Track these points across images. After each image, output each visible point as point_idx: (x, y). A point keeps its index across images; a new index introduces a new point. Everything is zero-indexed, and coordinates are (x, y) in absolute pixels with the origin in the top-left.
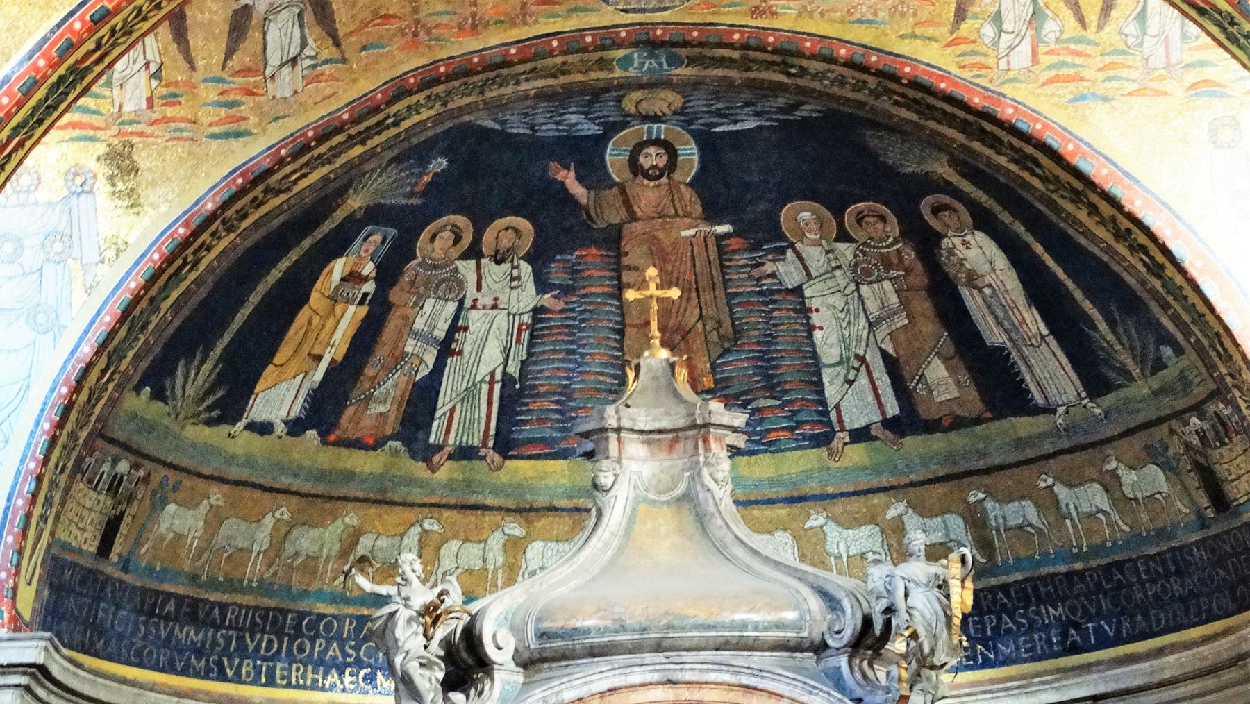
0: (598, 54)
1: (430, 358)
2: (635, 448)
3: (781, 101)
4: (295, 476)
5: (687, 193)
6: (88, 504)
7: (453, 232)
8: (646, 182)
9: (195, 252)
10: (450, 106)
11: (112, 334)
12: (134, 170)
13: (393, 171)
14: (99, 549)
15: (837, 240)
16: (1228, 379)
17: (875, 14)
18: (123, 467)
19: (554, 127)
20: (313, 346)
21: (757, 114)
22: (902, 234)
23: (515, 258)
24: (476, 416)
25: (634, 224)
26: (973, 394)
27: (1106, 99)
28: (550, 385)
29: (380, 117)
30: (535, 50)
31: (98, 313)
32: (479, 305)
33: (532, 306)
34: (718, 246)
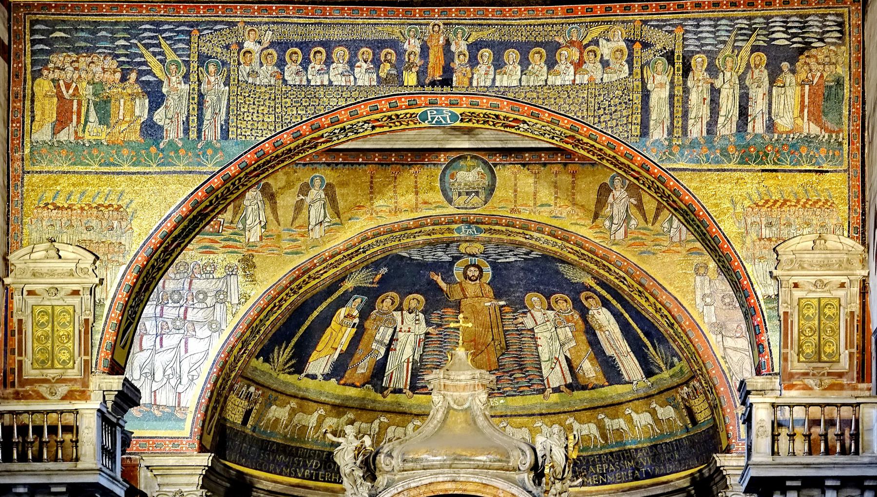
0: (447, 226)
1: (383, 351)
3: (524, 250)
4: (327, 396)
5: (488, 288)
6: (237, 404)
9: (279, 301)
10: (387, 245)
11: (243, 334)
13: (364, 273)
14: (242, 422)
15: (548, 309)
16: (698, 371)
17: (561, 214)
18: (252, 389)
21: (515, 255)
22: (574, 308)
26: (601, 376)
27: (654, 254)
29: (356, 249)
30: (420, 223)
31: (237, 325)
32: (403, 330)
34: (501, 311)
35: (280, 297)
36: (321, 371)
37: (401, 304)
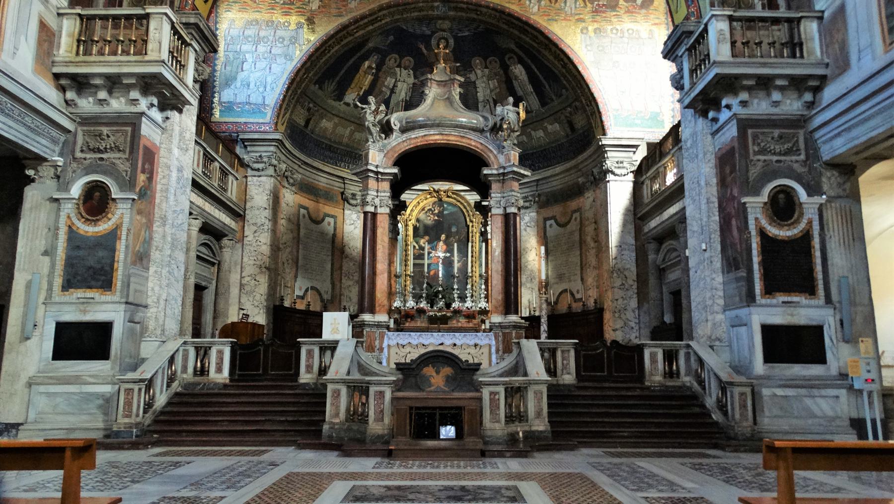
1: (388, 94)
2: (434, 85)
9: (329, 47)
12: (314, 23)
27: (556, 20)
29: (376, 16)
35: (329, 43)
37: (400, 62)
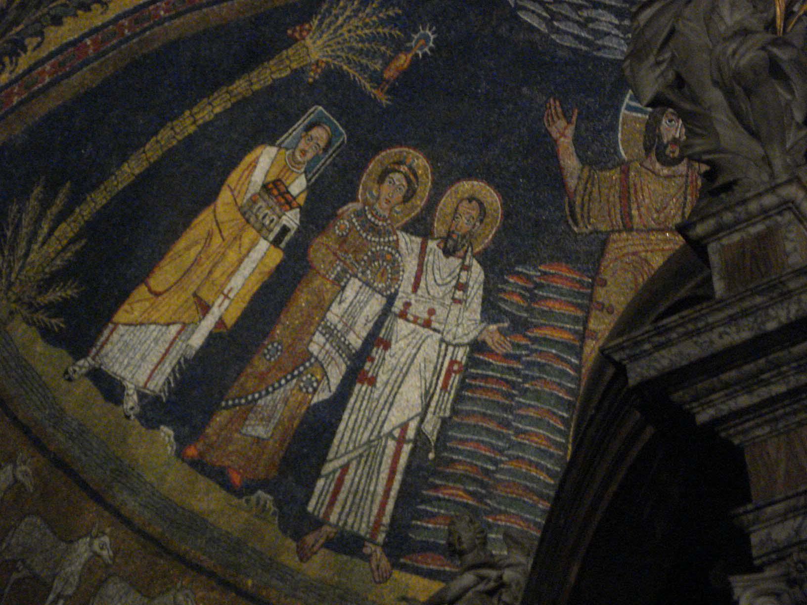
1: (336, 374)
7: (407, 177)
8: (658, 166)
19: (576, 31)
20: (203, 284)
23: (469, 254)
24: (372, 489)
25: (624, 235)
28: (471, 464)
32: (412, 310)
33: (472, 336)
36: (141, 378)
